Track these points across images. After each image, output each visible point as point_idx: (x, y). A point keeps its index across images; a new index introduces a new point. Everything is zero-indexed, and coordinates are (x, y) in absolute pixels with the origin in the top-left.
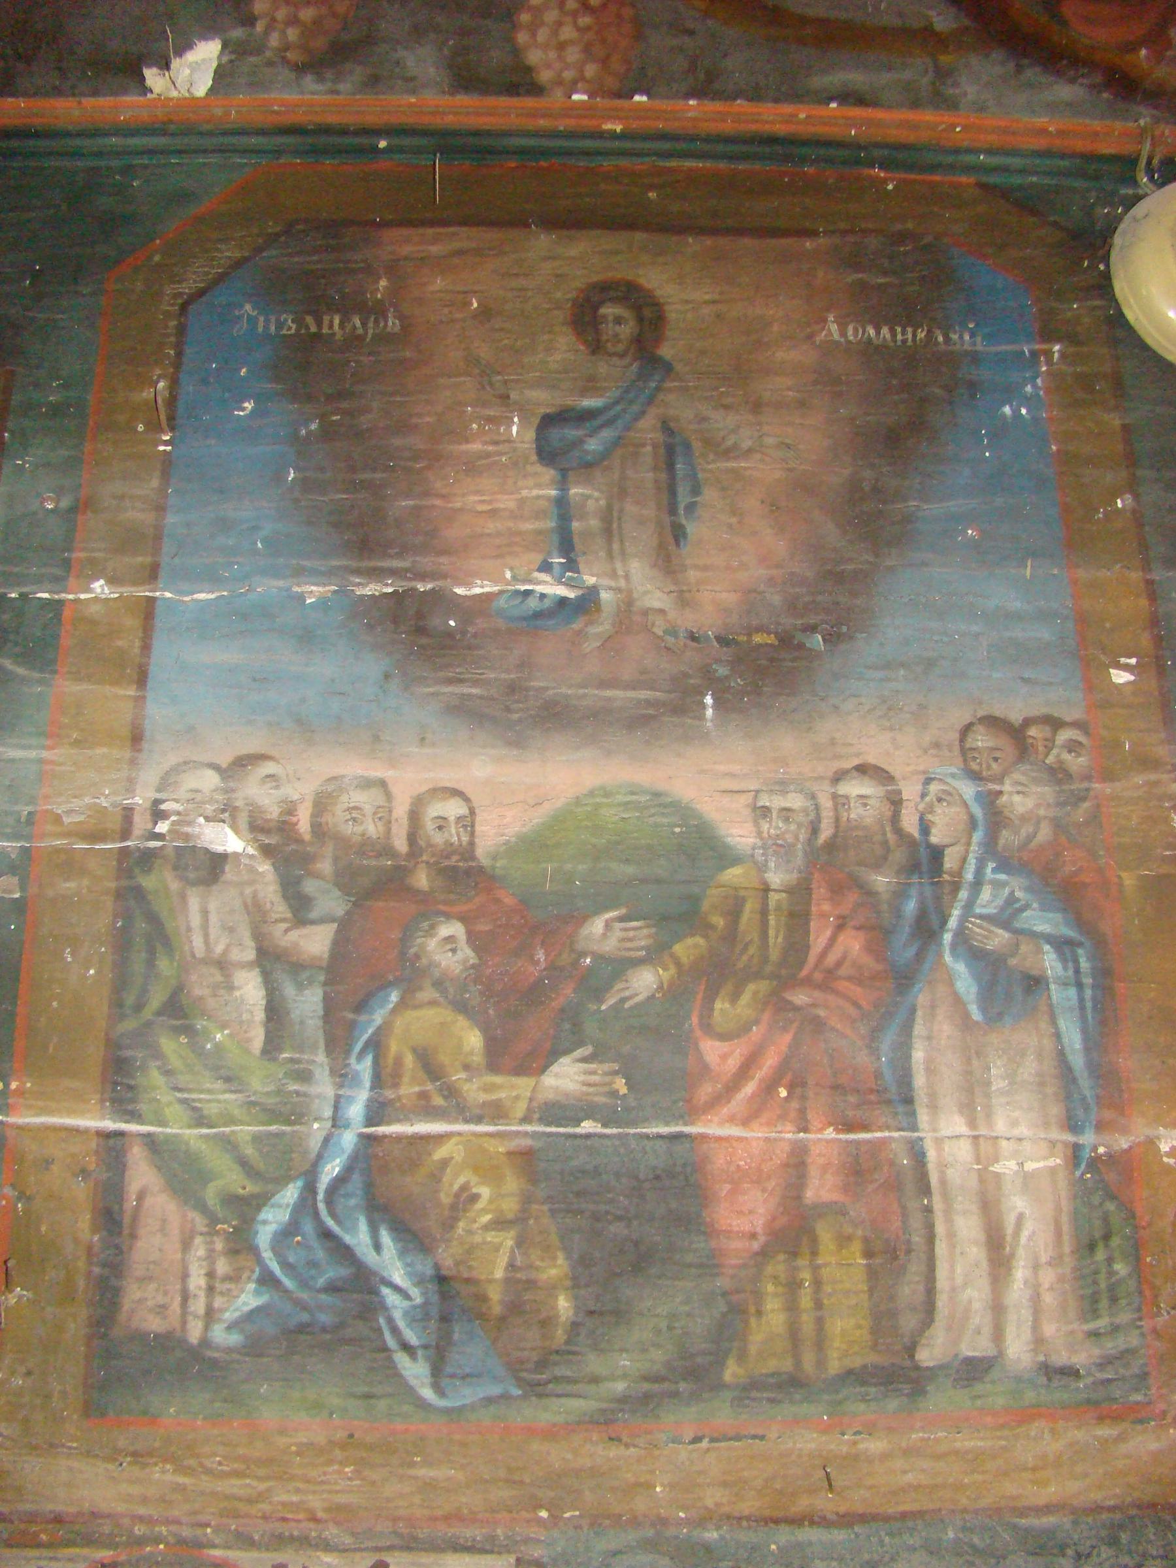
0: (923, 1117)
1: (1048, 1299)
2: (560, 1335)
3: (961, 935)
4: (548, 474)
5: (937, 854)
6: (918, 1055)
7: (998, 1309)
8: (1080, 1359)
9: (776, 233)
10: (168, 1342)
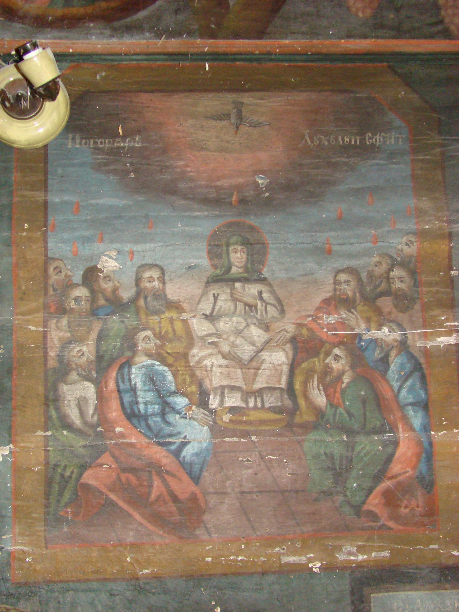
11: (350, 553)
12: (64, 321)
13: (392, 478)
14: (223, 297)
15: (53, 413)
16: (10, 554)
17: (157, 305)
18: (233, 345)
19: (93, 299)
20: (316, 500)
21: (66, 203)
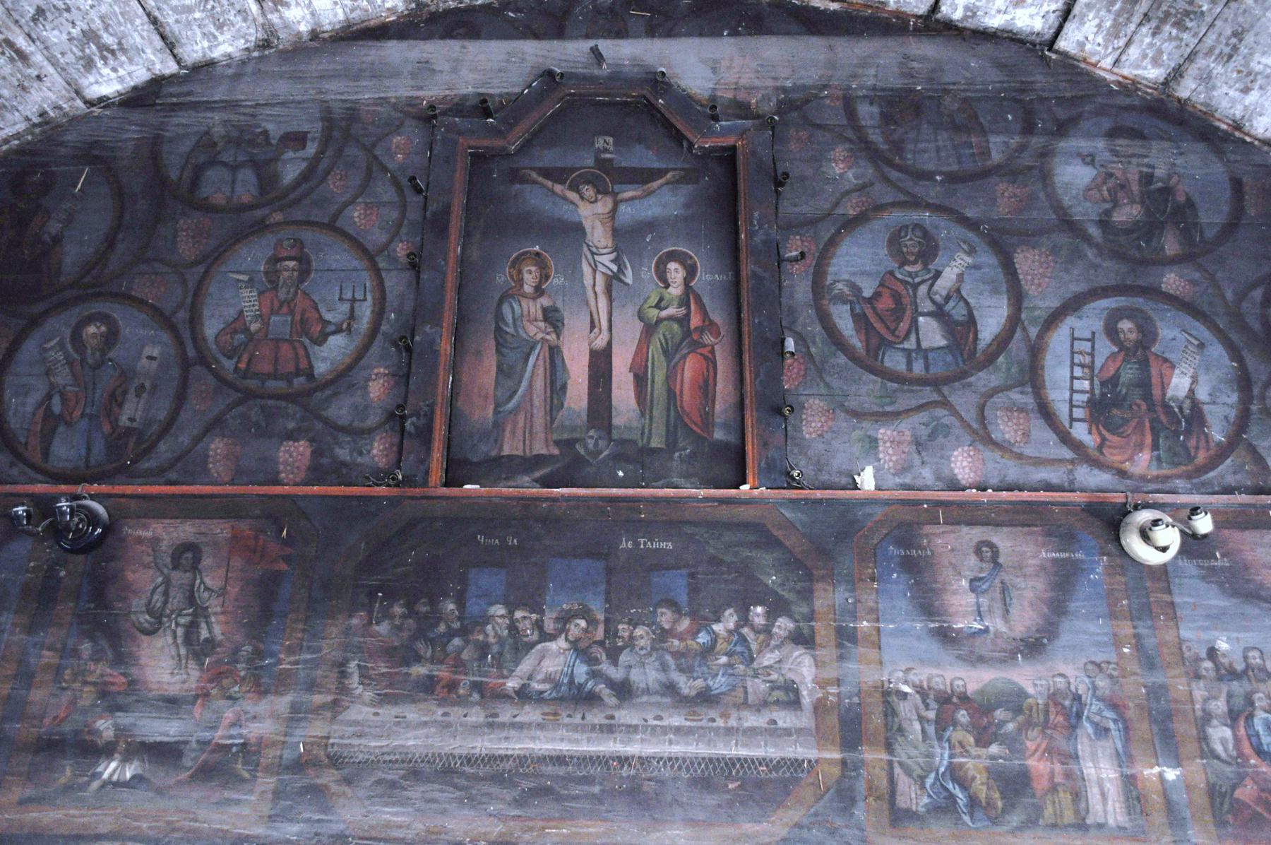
0: (1081, 761)
2: (999, 812)
3: (1088, 717)
4: (973, 595)
6: (1079, 747)
7: (1105, 812)
10: (908, 811)
17: (1262, 675)
19: (1217, 670)
21: (1188, 603)
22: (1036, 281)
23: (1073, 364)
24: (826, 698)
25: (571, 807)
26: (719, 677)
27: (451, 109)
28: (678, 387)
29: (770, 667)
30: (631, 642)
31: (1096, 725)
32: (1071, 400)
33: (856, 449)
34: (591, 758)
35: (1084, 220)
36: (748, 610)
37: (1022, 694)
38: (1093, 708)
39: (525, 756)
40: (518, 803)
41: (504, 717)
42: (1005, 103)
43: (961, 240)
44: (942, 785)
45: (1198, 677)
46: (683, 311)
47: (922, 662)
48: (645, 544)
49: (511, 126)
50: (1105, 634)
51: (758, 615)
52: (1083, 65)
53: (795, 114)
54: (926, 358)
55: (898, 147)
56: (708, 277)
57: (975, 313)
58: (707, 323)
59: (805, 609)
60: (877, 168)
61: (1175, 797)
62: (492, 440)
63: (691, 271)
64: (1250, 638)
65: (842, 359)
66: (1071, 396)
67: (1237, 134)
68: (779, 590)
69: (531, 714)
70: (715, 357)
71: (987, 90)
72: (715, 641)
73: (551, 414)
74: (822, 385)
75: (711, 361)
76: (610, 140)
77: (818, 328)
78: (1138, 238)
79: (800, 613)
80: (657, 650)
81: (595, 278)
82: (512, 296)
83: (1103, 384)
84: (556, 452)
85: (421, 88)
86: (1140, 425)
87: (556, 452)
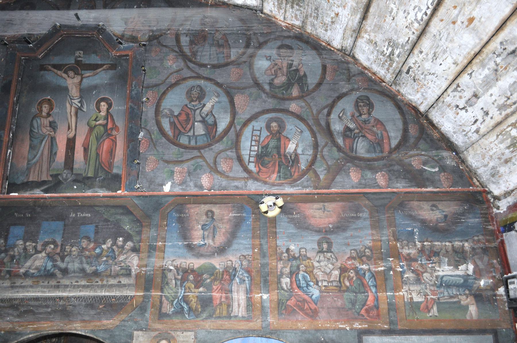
0: (233, 293)
1: (243, 310)
3: (238, 276)
4: (202, 231)
5: (236, 268)
6: (233, 287)
7: (238, 311)
8: (246, 316)
9: (226, 204)
10: (166, 313)
11: (357, 325)
12: (282, 262)
13: (367, 305)
14: (321, 256)
15: (279, 286)
16: (270, 322)
17: (305, 258)
18: (325, 269)
19: (288, 257)
20: (348, 311)
21: (281, 232)
22: (242, 108)
23: (252, 140)
24: (141, 272)
25: (39, 317)
26: (102, 266)
27: (16, 41)
28: (101, 152)
29: (122, 261)
30: (70, 254)
31: (240, 279)
32: (250, 155)
33: (165, 176)
34: (49, 298)
35: (263, 83)
36: (116, 239)
37: (214, 268)
38: (240, 272)
39: (23, 298)
40: (19, 316)
41: (18, 284)
42: (240, 35)
43: (215, 91)
44: (180, 304)
45: (281, 259)
46: (105, 122)
47: (179, 257)
48: (80, 214)
49: (38, 48)
50: (249, 244)
51: (120, 241)
52: (273, 19)
53: (155, 41)
54: (196, 139)
55: (194, 54)
56: (116, 108)
57: (217, 120)
58: (114, 126)
59: (138, 238)
60: (185, 62)
61: (265, 305)
62: (25, 175)
63: (110, 106)
64: (301, 244)
65: (164, 140)
66: (250, 152)
67: (329, 47)
68: (129, 231)
69: (28, 282)
70: (116, 140)
71: (234, 30)
72: (102, 252)
73: (50, 164)
74: (155, 150)
75: (114, 142)
76: (82, 52)
77: (156, 128)
78: (283, 90)
79: (136, 240)
80: (80, 256)
81: (71, 109)
82: (38, 117)
83: (262, 148)
84: (50, 179)
85: (6, 32)
86: (274, 165)
87: (50, 179)
